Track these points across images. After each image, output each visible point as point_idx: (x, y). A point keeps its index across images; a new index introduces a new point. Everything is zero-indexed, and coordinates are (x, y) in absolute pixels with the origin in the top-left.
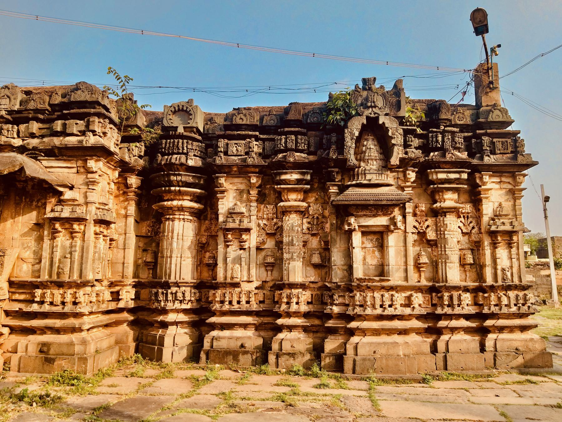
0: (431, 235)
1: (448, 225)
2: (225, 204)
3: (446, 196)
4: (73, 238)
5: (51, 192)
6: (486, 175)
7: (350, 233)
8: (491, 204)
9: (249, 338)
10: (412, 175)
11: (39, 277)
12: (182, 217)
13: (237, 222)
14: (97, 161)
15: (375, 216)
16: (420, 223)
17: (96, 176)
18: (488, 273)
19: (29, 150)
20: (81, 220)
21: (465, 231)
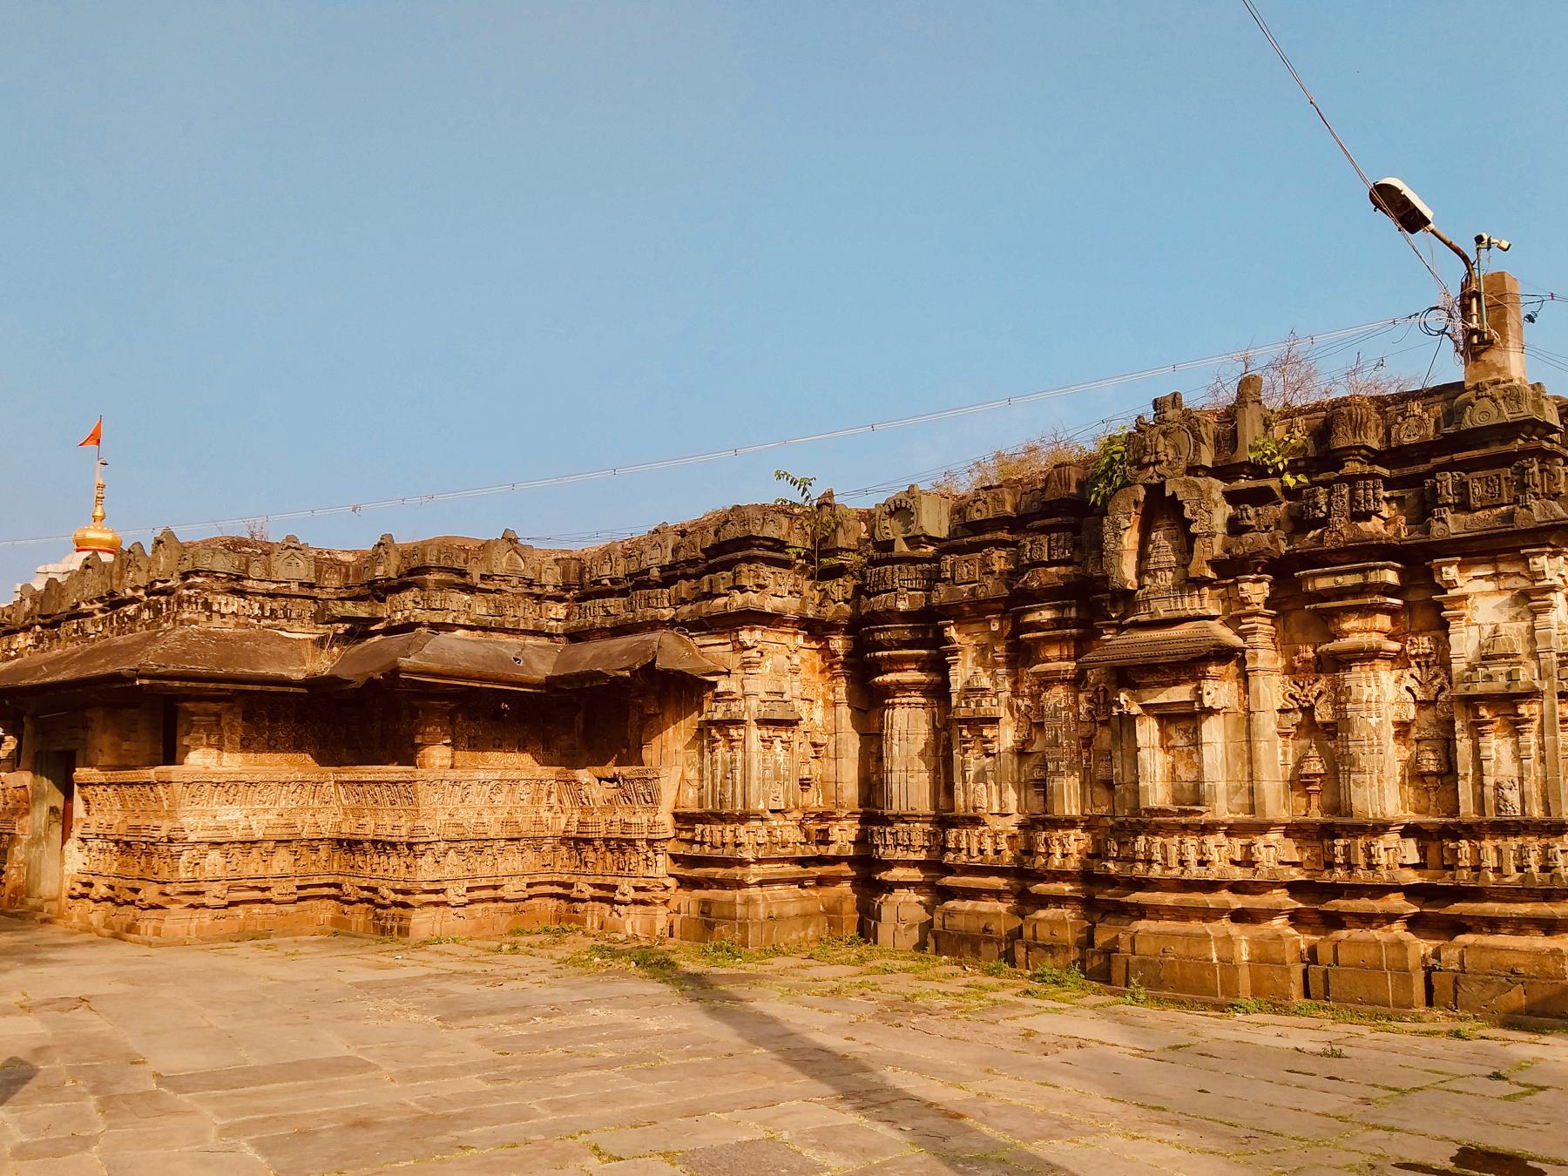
0: (1323, 713)
1: (1354, 689)
2: (962, 672)
3: (1346, 626)
4: (732, 748)
6: (1449, 564)
7: (1129, 721)
8: (1474, 630)
9: (998, 914)
10: (1256, 591)
12: (904, 700)
13: (973, 705)
14: (752, 630)
15: (1166, 685)
16: (1302, 688)
17: (754, 653)
18: (1465, 790)
19: (677, 624)
20: (738, 723)
21: (1420, 696)
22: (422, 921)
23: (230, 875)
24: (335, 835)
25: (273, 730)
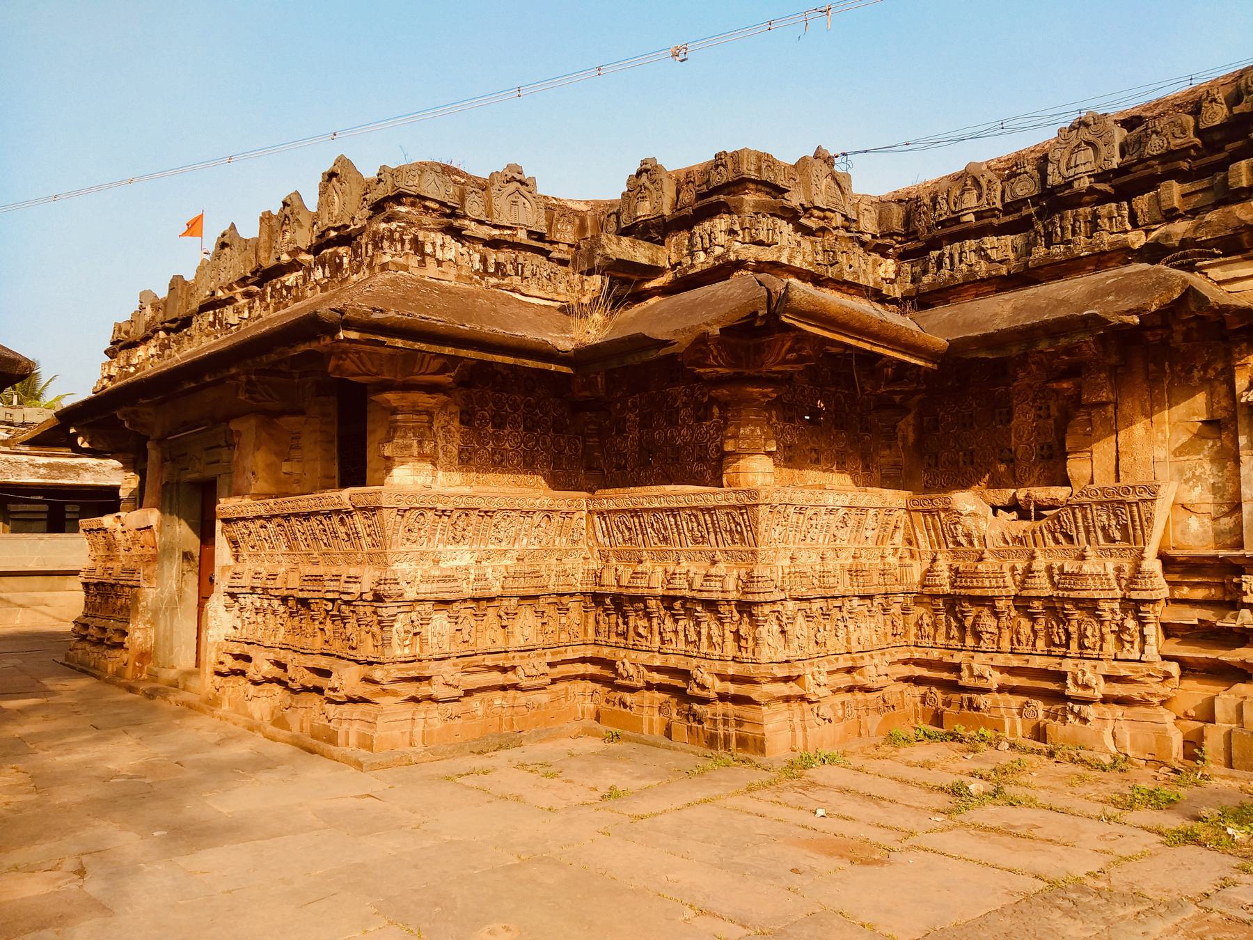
5: (1244, 341)
11: (1240, 545)
19: (1172, 249)
22: (777, 725)
23: (463, 649)
24: (590, 588)
25: (498, 439)
